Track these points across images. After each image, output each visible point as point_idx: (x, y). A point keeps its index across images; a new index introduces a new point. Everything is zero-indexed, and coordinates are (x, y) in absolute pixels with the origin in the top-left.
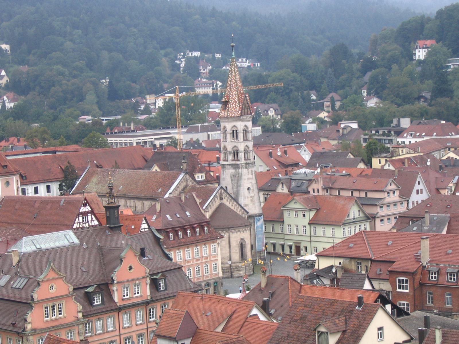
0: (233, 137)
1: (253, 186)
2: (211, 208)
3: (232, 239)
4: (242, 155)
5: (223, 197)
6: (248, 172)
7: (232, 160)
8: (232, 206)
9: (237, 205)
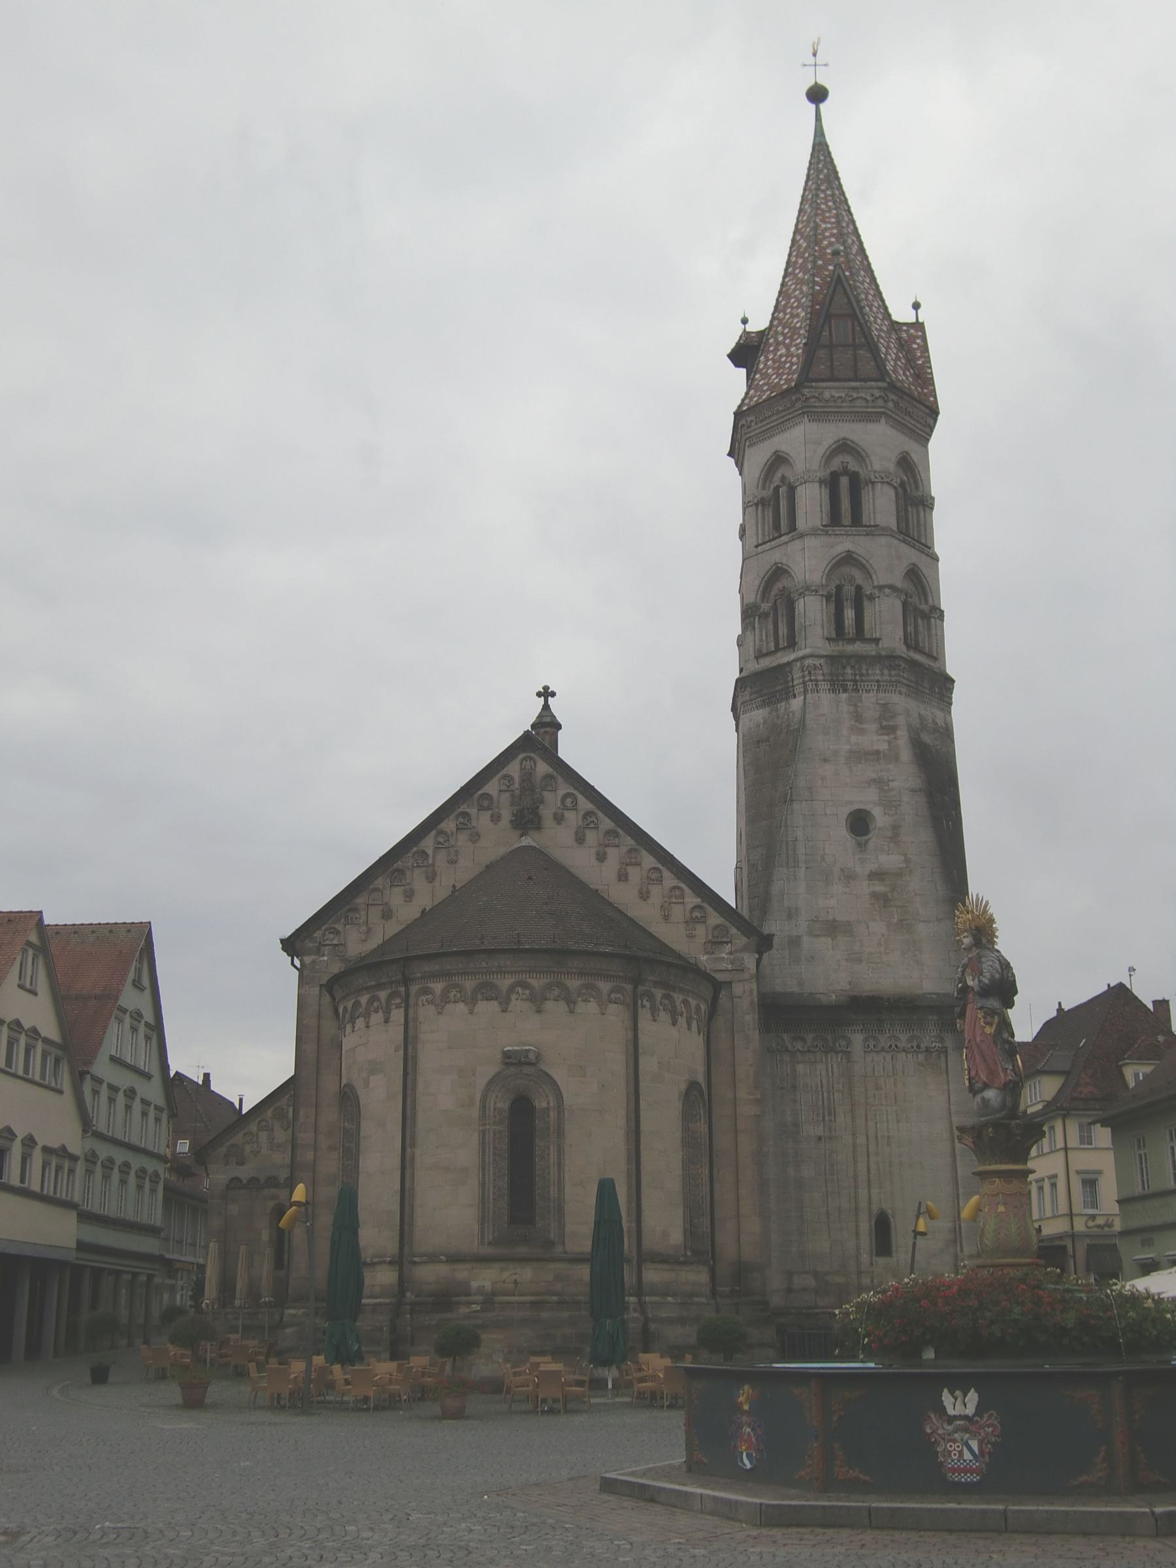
1: (890, 805)
2: (431, 877)
3: (429, 1058)
5: (547, 812)
6: (858, 717)
8: (623, 877)
9: (667, 874)
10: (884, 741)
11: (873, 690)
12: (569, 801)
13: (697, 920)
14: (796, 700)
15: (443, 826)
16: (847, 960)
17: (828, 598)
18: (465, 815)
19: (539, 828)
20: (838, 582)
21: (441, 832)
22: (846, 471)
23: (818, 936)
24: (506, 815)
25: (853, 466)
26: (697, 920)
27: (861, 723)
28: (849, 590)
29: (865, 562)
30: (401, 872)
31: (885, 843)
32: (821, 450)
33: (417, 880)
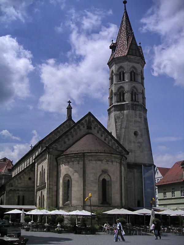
0: (120, 79)
1: (141, 131)
3: (88, 171)
4: (127, 96)
5: (93, 127)
6: (136, 115)
7: (117, 102)
9: (113, 140)
12: (96, 125)
15: (75, 127)
18: (79, 126)
19: (91, 129)
21: (75, 129)
22: (133, 72)
24: (86, 126)
25: (135, 71)
30: (67, 135)
32: (130, 67)
33: (70, 137)
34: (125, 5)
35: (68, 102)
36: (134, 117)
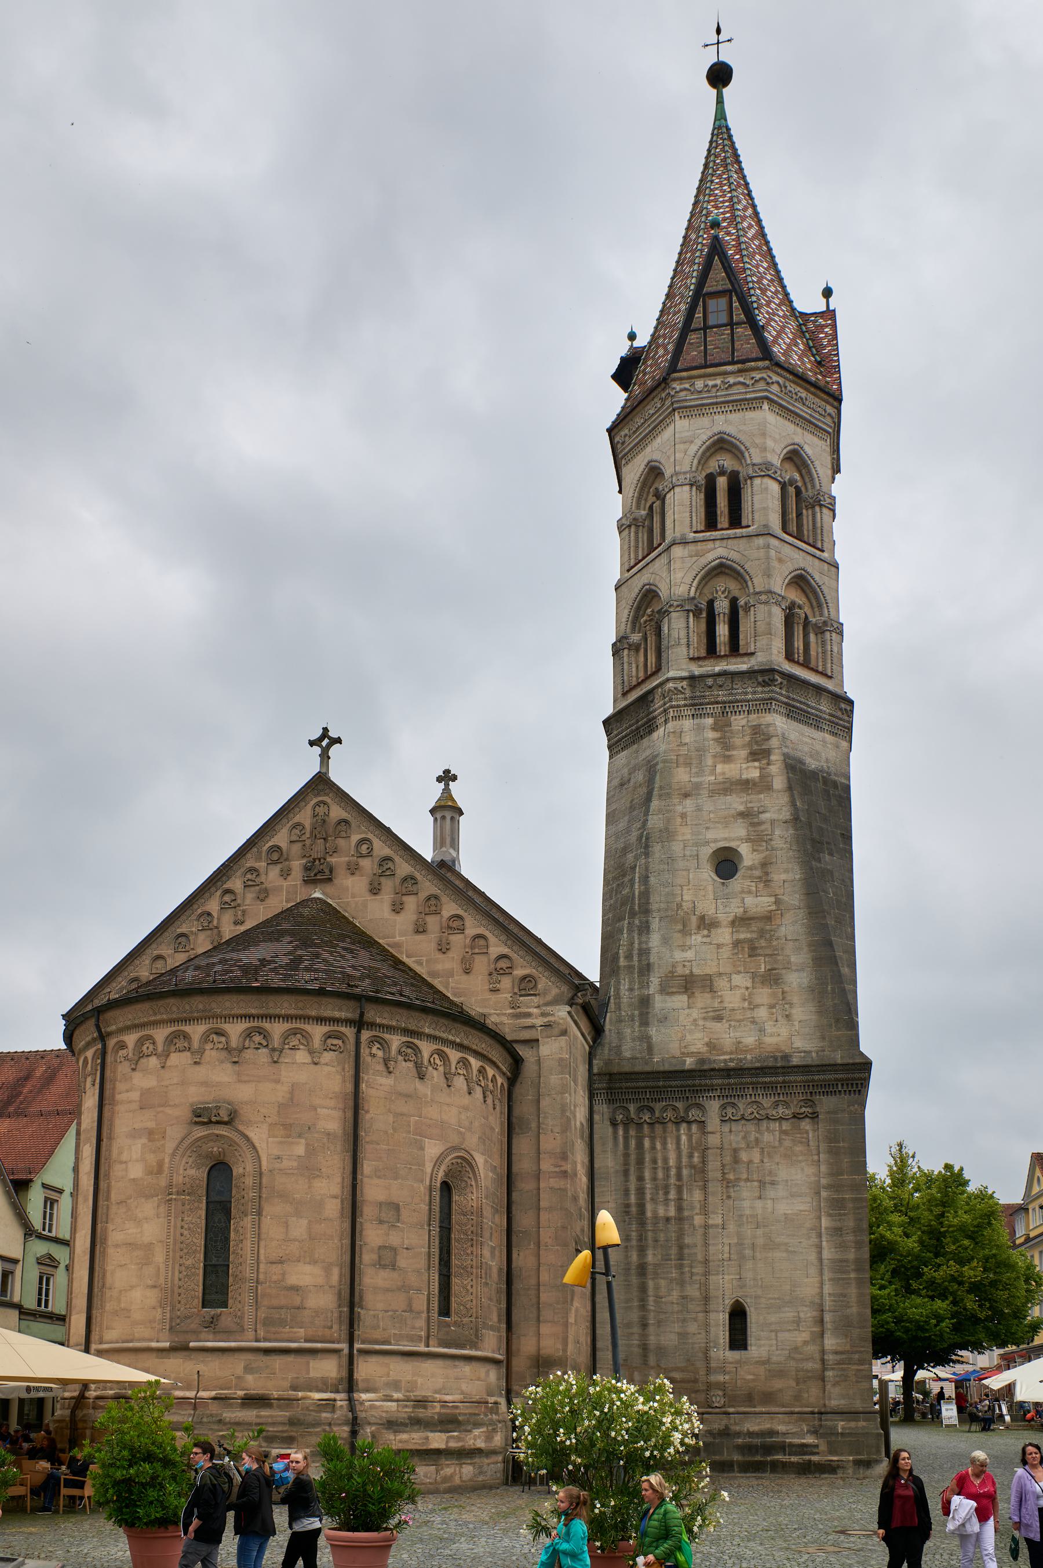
1: (757, 839)
6: (725, 744)
10: (755, 768)
11: (744, 711)
13: (501, 972)
14: (657, 732)
16: (704, 1019)
17: (697, 613)
20: (710, 598)
23: (673, 993)
26: (501, 972)
27: (727, 750)
28: (722, 606)
29: (739, 568)
31: (753, 884)
34: (720, 101)
35: (439, 779)
36: (710, 762)
